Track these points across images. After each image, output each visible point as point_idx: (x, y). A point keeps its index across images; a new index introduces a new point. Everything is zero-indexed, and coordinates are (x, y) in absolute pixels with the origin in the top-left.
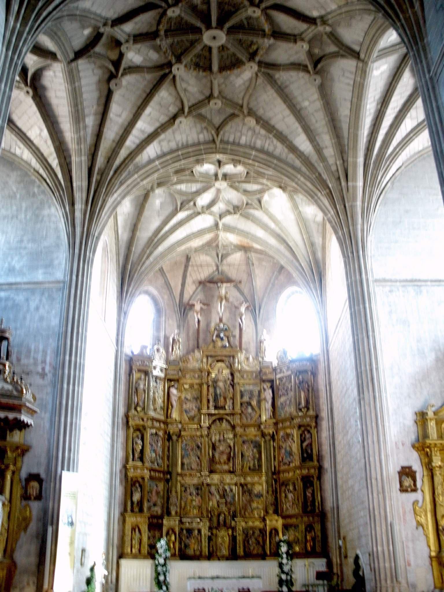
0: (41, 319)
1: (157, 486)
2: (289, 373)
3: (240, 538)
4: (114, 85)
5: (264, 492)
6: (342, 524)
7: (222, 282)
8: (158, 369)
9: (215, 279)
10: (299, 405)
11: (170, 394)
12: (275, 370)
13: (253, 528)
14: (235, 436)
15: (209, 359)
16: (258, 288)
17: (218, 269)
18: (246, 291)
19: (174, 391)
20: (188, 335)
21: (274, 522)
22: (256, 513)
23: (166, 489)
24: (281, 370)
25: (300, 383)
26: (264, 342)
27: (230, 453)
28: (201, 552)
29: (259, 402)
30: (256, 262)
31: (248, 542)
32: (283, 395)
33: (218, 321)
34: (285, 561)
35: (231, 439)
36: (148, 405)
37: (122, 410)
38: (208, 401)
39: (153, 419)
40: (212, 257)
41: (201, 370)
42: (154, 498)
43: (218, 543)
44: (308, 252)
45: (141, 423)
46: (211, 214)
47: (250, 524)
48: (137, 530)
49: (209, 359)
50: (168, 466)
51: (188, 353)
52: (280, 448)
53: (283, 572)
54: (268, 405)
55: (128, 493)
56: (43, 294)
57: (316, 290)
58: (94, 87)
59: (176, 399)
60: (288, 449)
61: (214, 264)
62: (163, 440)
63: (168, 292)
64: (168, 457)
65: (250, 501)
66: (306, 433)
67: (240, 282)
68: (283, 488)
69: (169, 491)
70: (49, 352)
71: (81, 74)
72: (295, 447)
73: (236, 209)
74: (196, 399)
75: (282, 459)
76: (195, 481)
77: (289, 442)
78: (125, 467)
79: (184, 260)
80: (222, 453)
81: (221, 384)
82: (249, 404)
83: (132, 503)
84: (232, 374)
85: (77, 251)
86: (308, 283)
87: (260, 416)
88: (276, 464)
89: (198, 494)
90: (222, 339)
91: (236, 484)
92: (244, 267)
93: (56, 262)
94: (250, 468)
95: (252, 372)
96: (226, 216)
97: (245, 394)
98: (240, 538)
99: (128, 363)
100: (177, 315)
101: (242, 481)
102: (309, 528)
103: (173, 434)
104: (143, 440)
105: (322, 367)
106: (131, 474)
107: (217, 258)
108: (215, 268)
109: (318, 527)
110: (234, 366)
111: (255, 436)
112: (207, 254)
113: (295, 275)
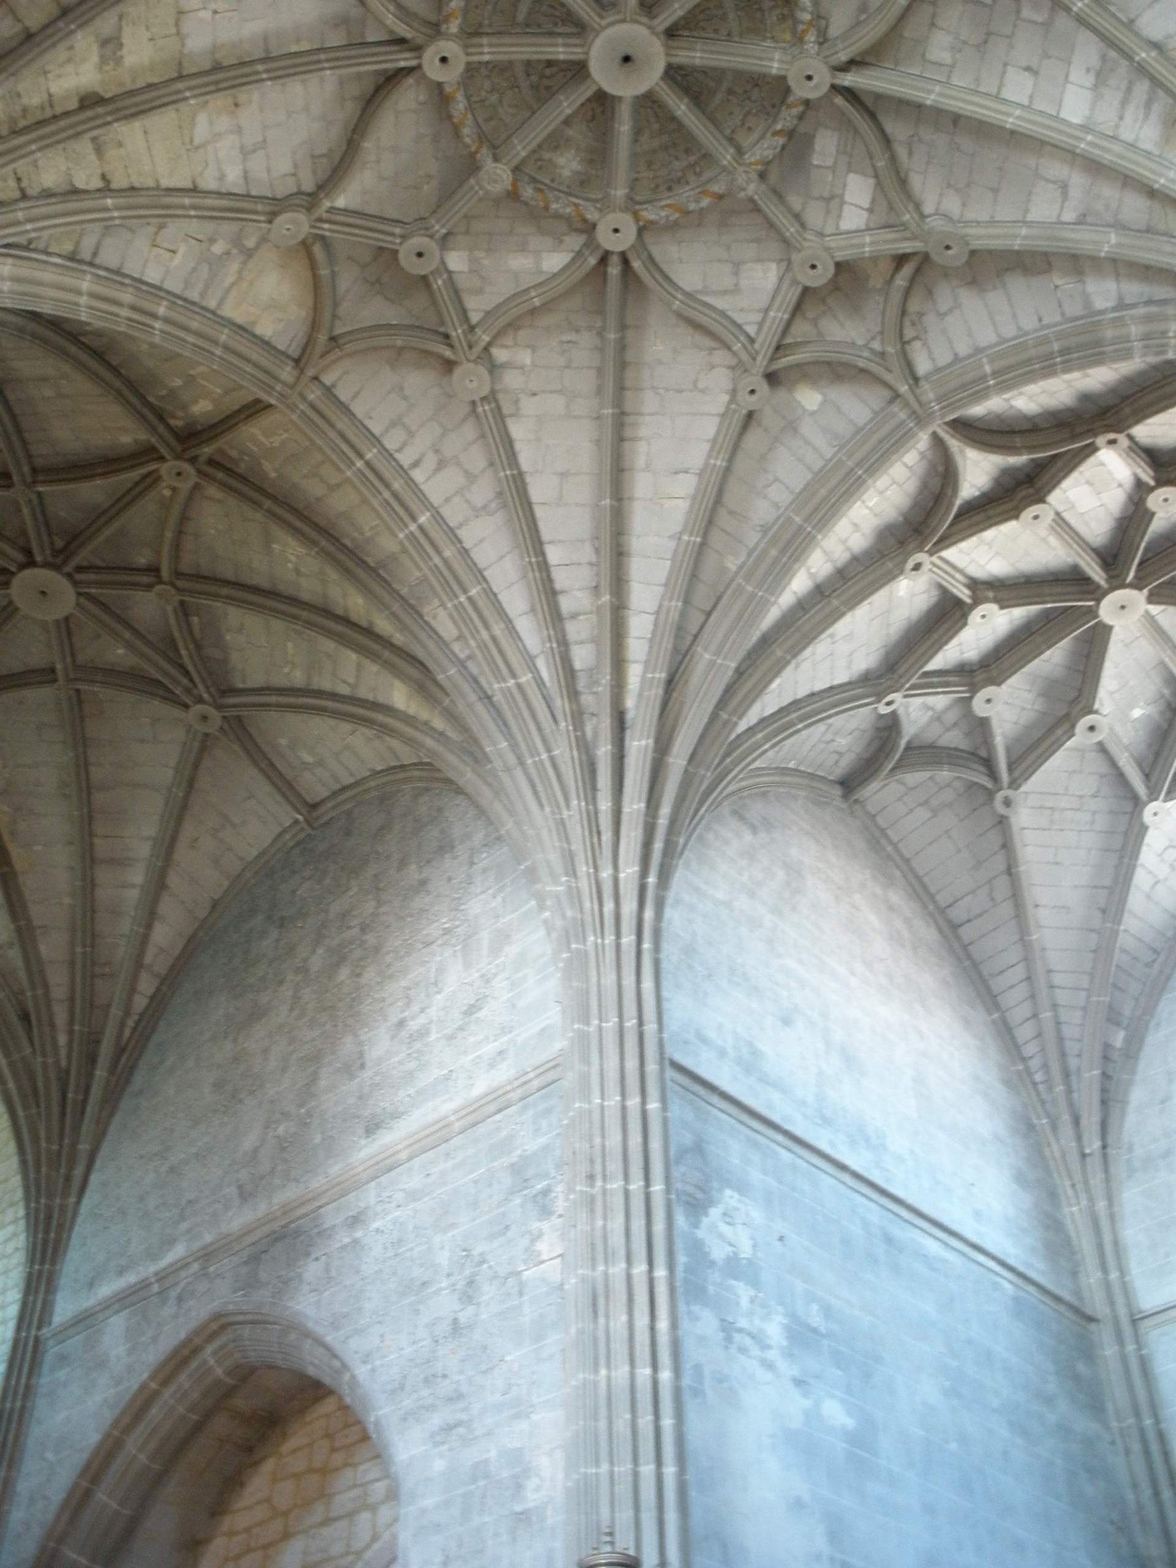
4: (950, 252)
58: (995, 298)
71: (963, 349)
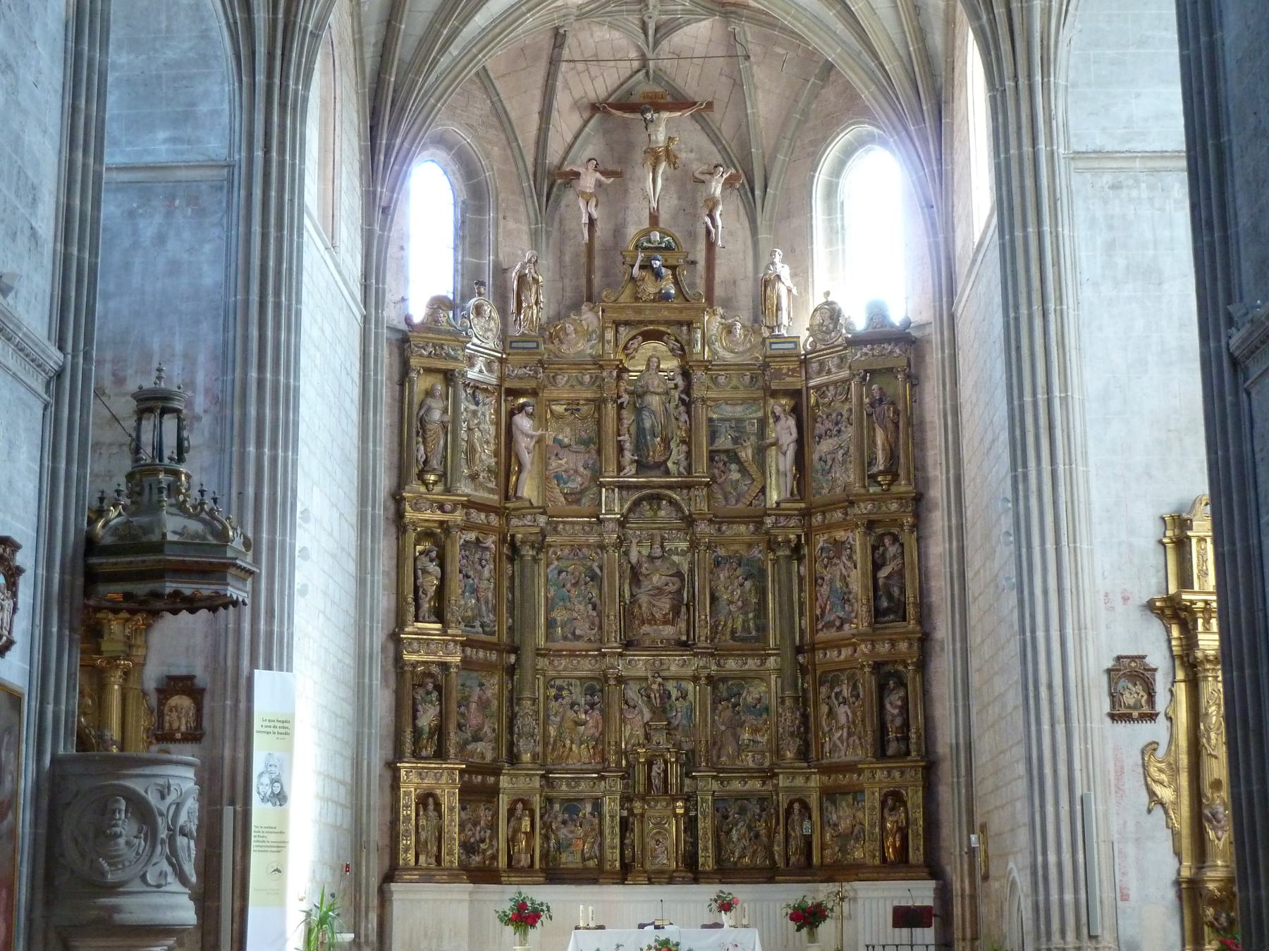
0: (175, 268)
1: (481, 685)
2: (845, 374)
5: (774, 702)
6: (979, 791)
7: (658, 108)
8: (480, 363)
9: (635, 99)
10: (870, 464)
12: (805, 362)
14: (694, 545)
15: (621, 329)
16: (762, 121)
17: (644, 65)
18: (727, 131)
19: (523, 423)
20: (560, 261)
22: (750, 759)
24: (822, 364)
25: (872, 405)
27: (680, 591)
28: (601, 860)
30: (755, 49)
31: (729, 832)
32: (828, 434)
33: (646, 225)
35: (683, 553)
37: (384, 482)
38: (621, 449)
39: (470, 505)
40: (628, 33)
41: (598, 363)
42: (474, 718)
47: (737, 786)
48: (431, 807)
49: (621, 329)
50: (511, 629)
51: (559, 317)
52: (816, 580)
55: (404, 709)
56: (171, 198)
57: (926, 140)
60: (838, 584)
61: (633, 54)
62: (497, 559)
65: (735, 726)
66: (887, 541)
67: (710, 105)
69: (514, 699)
70: (202, 358)
72: (857, 582)
74: (586, 443)
76: (586, 667)
78: (395, 638)
79: (546, 41)
80: (659, 591)
81: (654, 401)
82: (733, 456)
83: (417, 732)
84: (686, 374)
85: (261, 78)
87: (763, 490)
88: (806, 622)
89: (592, 706)
90: (658, 275)
91: (695, 679)
93: (204, 108)
94: (733, 632)
95: (739, 367)
97: (723, 428)
99: (396, 351)
100: (529, 201)
102: (894, 799)
103: (523, 542)
105: (934, 360)
107: (642, 36)
109: (915, 798)
110: (691, 353)
111: (750, 545)
112: (612, 26)
113: (867, 94)
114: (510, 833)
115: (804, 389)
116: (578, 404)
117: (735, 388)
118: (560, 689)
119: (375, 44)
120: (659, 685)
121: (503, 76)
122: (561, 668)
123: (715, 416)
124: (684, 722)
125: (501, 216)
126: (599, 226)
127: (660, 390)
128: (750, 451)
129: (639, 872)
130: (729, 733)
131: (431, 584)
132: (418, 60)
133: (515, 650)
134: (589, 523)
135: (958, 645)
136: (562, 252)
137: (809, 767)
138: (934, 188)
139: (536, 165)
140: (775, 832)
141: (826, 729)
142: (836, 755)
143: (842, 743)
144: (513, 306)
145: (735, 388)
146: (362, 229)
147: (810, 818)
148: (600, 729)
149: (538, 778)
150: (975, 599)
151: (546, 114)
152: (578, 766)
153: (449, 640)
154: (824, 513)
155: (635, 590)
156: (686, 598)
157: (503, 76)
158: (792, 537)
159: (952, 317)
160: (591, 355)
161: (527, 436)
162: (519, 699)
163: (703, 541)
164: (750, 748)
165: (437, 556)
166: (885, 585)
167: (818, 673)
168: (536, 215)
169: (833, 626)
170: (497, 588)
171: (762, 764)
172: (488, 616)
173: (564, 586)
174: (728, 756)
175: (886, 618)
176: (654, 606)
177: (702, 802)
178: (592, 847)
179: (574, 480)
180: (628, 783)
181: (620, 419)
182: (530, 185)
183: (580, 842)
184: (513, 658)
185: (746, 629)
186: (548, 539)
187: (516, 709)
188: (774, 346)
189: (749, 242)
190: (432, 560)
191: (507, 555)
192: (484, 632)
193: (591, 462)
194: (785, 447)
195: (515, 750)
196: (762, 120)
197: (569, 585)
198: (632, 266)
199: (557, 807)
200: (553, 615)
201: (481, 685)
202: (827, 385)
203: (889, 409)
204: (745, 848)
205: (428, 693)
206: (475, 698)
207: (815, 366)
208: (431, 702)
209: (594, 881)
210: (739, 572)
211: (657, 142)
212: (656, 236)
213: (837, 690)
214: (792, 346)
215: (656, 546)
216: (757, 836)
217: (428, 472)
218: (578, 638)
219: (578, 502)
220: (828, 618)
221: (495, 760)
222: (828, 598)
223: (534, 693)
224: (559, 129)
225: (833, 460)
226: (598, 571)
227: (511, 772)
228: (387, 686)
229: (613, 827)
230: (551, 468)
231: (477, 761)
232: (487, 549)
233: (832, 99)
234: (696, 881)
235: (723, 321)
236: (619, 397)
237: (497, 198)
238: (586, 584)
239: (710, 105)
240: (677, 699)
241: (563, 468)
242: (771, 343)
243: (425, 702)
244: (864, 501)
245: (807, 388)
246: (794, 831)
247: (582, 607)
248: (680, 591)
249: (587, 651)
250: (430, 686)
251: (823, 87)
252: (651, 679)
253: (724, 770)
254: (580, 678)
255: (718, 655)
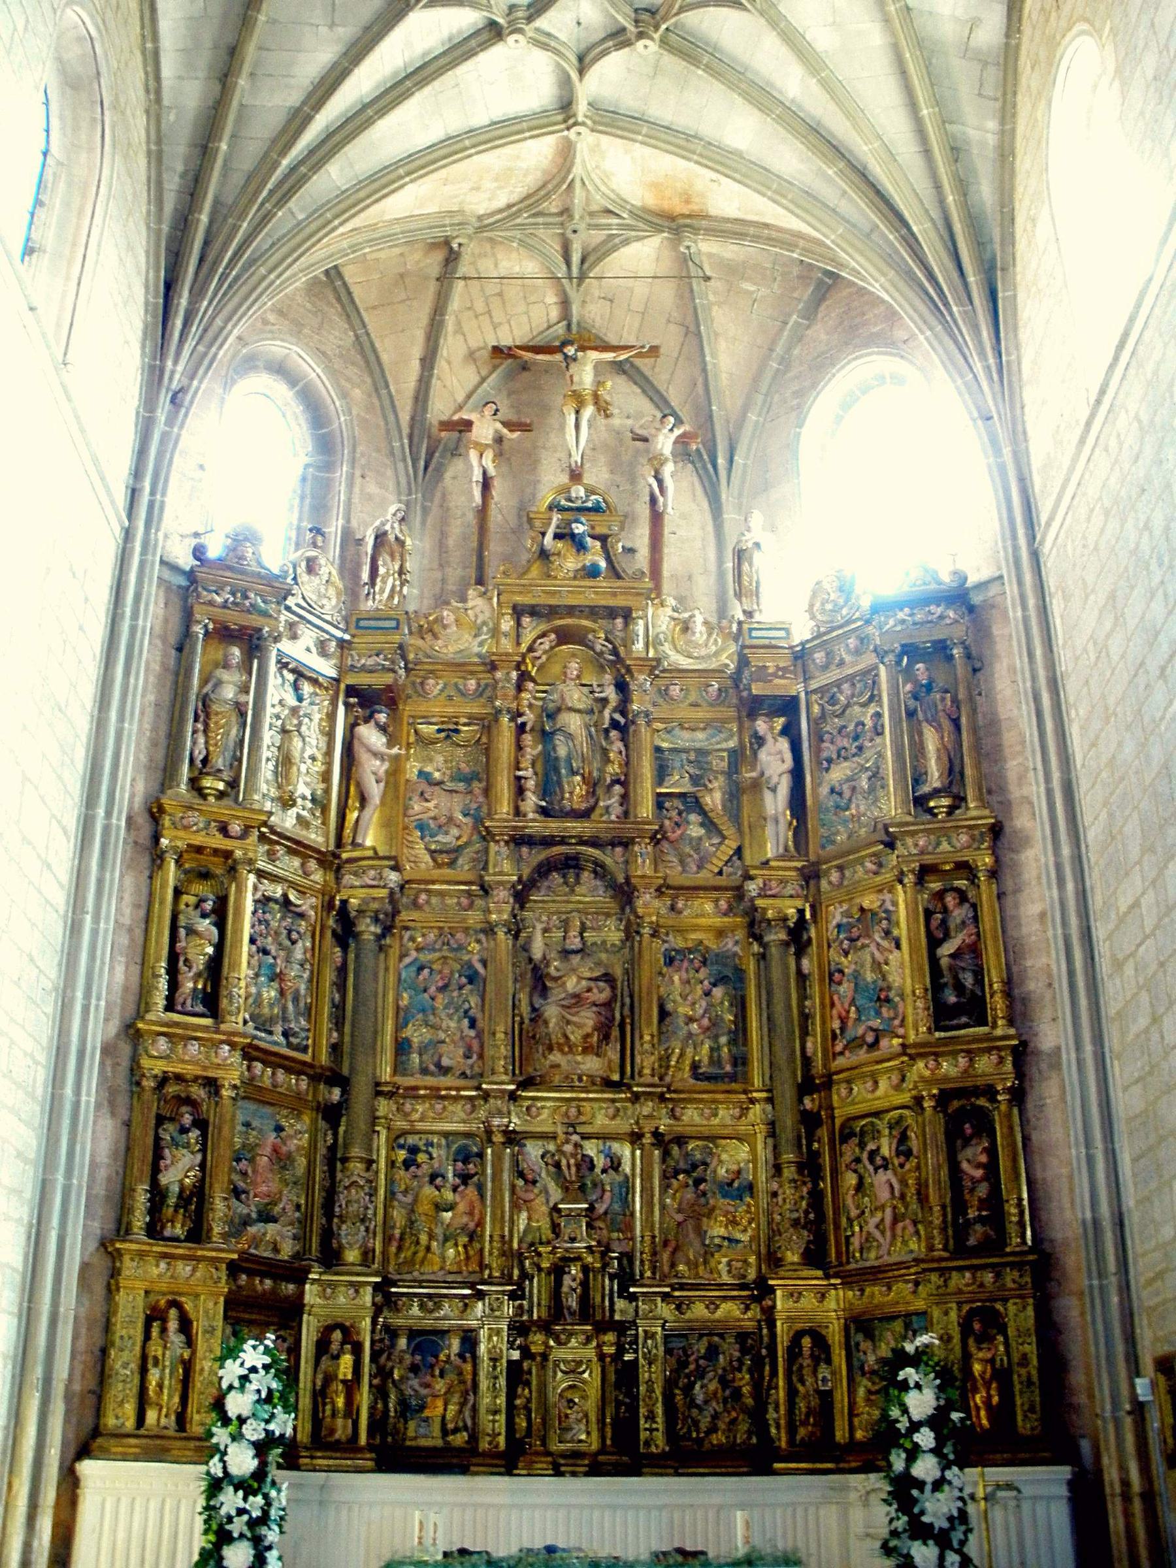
1: (279, 1129)
2: (870, 659)
3: (652, 1376)
5: (762, 1177)
7: (582, 348)
11: (356, 743)
12: (801, 656)
13: (708, 1330)
14: (631, 932)
15: (526, 620)
21: (809, 1301)
22: (723, 1267)
23: (322, 1151)
26: (757, 557)
28: (474, 1438)
29: (735, 794)
31: (688, 1390)
32: (843, 755)
33: (564, 479)
34: (925, 1468)
36: (253, 771)
38: (520, 791)
42: (266, 1184)
43: (553, 1398)
44: (938, 187)
45: (218, 841)
46: (544, 42)
47: (699, 1311)
48: (173, 1325)
49: (526, 620)
50: (336, 1048)
53: (920, 1531)
54: (776, 803)
57: (975, 328)
59: (382, 768)
60: (869, 976)
63: (369, 380)
64: (339, 1009)
66: (950, 900)
68: (849, 1151)
69: (335, 1158)
73: (645, 17)
74: (468, 779)
75: (843, 1021)
76: (456, 1119)
77: (874, 945)
78: (132, 1033)
80: (577, 999)
81: (574, 723)
82: (692, 802)
86: (937, 306)
89: (465, 1178)
90: (580, 547)
91: (635, 1138)
92: (667, 294)
94: (695, 1066)
96: (605, 53)
97: (676, 761)
98: (652, 1376)
100: (400, 465)
101: (664, 1124)
103: (360, 912)
104: (220, 914)
106: (154, 1066)
107: (564, 267)
108: (554, 313)
110: (629, 651)
111: (720, 933)
114: (319, 1383)
115: (803, 695)
116: (457, 724)
117: (695, 705)
118: (414, 1150)
119: (183, 176)
120: (576, 1145)
121: (374, 308)
122: (416, 1116)
123: (665, 745)
124: (617, 1207)
125: (358, 473)
126: (496, 492)
127: (581, 706)
128: (718, 795)
129: (537, 1454)
130: (690, 1226)
131: (200, 952)
132: (244, 201)
133: (343, 1082)
134: (468, 892)
135: (1088, 1048)
136: (443, 535)
137: (827, 1277)
138: (991, 388)
139: (412, 427)
140: (770, 1388)
141: (854, 1213)
142: (873, 1255)
143: (883, 1233)
144: (365, 576)
145: (695, 705)
146: (138, 413)
147: (829, 1361)
148: (476, 1218)
149: (369, 1289)
150: (1118, 965)
151: (428, 361)
152: (440, 1276)
153: (222, 1042)
154: (841, 868)
155: (538, 1002)
156: (618, 1016)
157: (374, 308)
158: (791, 912)
159: (1035, 555)
160: (479, 655)
161: (376, 754)
162: (345, 1160)
163: (647, 919)
164: (724, 1250)
165: (213, 911)
166: (951, 968)
167: (838, 1122)
168: (409, 483)
169: (861, 1046)
170: (315, 981)
171: (744, 1277)
172: (297, 1021)
173: (425, 991)
174: (688, 1263)
175: (955, 1022)
176: (568, 1022)
177: (646, 1338)
178: (460, 1411)
179: (447, 833)
180: (521, 1306)
181: (519, 748)
182: (402, 445)
183: (440, 1403)
184: (336, 1094)
185: (715, 1061)
186: (404, 916)
187: (339, 1175)
188: (754, 634)
189: (710, 528)
190: (204, 916)
191: (334, 933)
192: (289, 1045)
193: (474, 806)
194: (775, 779)
195: (335, 1245)
196: (724, 376)
197: (433, 989)
198: (543, 534)
199: (402, 1342)
200: (408, 1032)
201: (279, 1129)
202: (838, 684)
203: (943, 699)
204: (715, 1416)
205: (184, 1130)
206: (268, 1150)
207: (819, 657)
208: (187, 1146)
209: (463, 1470)
210: (702, 974)
211: (581, 383)
212: (579, 491)
213: (871, 1146)
214: (782, 634)
215: (573, 933)
216: (737, 1394)
217: (208, 774)
218: (445, 1071)
219: (452, 864)
220: (850, 1033)
221: (297, 1256)
222: (853, 1002)
223: (369, 1149)
224: (448, 384)
225: (854, 789)
226: (479, 967)
227: (324, 1277)
228: (113, 1114)
229: (496, 1378)
230: (411, 812)
231: (266, 1254)
232: (301, 916)
233: (823, 337)
234: (633, 1468)
235: (676, 615)
236: (520, 715)
237: (354, 451)
238: (461, 988)
239: (654, 350)
240: (604, 1171)
241: (432, 814)
242: (751, 630)
243: (177, 1145)
244: (913, 834)
245: (807, 693)
246: (803, 1384)
247: (453, 1024)
248: (608, 1004)
249: (458, 1089)
250: (187, 1119)
251: (808, 327)
252: (562, 1137)
253: (682, 1287)
254: (446, 1135)
255: (671, 1099)
